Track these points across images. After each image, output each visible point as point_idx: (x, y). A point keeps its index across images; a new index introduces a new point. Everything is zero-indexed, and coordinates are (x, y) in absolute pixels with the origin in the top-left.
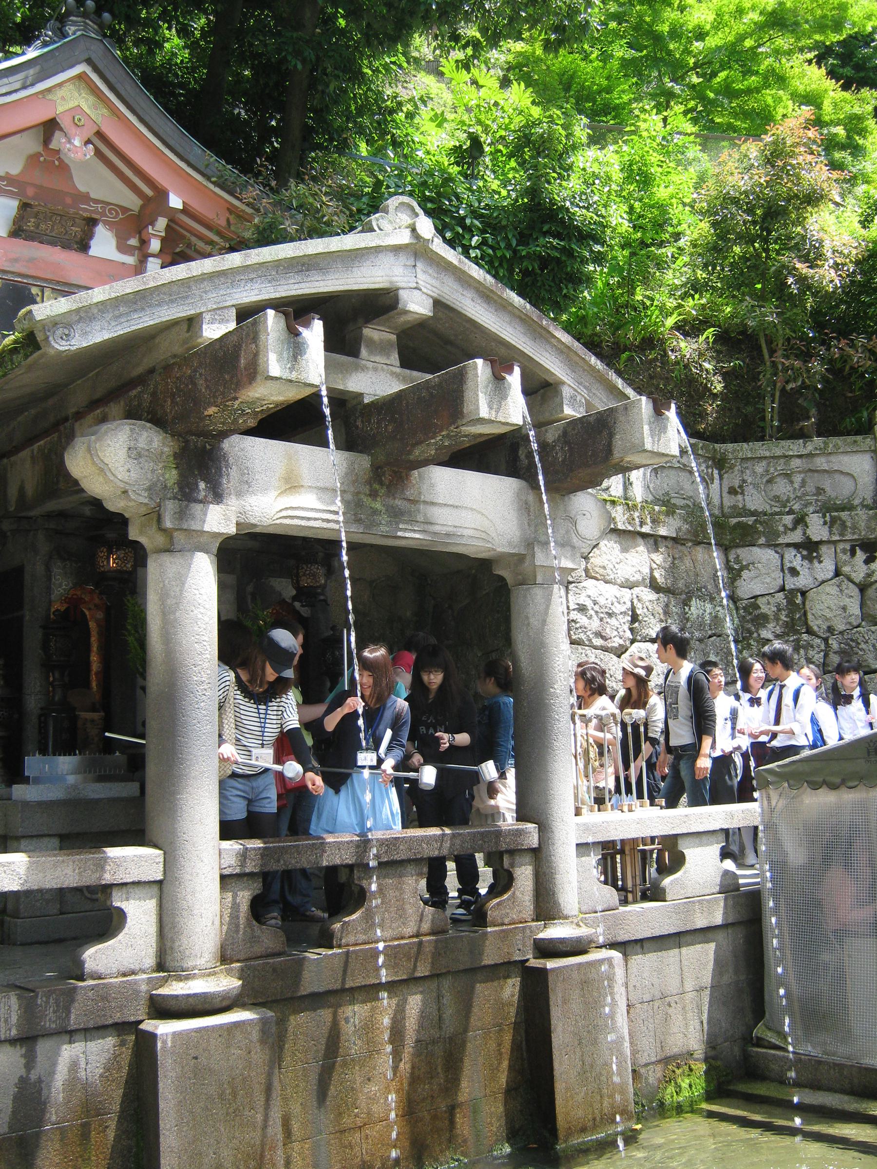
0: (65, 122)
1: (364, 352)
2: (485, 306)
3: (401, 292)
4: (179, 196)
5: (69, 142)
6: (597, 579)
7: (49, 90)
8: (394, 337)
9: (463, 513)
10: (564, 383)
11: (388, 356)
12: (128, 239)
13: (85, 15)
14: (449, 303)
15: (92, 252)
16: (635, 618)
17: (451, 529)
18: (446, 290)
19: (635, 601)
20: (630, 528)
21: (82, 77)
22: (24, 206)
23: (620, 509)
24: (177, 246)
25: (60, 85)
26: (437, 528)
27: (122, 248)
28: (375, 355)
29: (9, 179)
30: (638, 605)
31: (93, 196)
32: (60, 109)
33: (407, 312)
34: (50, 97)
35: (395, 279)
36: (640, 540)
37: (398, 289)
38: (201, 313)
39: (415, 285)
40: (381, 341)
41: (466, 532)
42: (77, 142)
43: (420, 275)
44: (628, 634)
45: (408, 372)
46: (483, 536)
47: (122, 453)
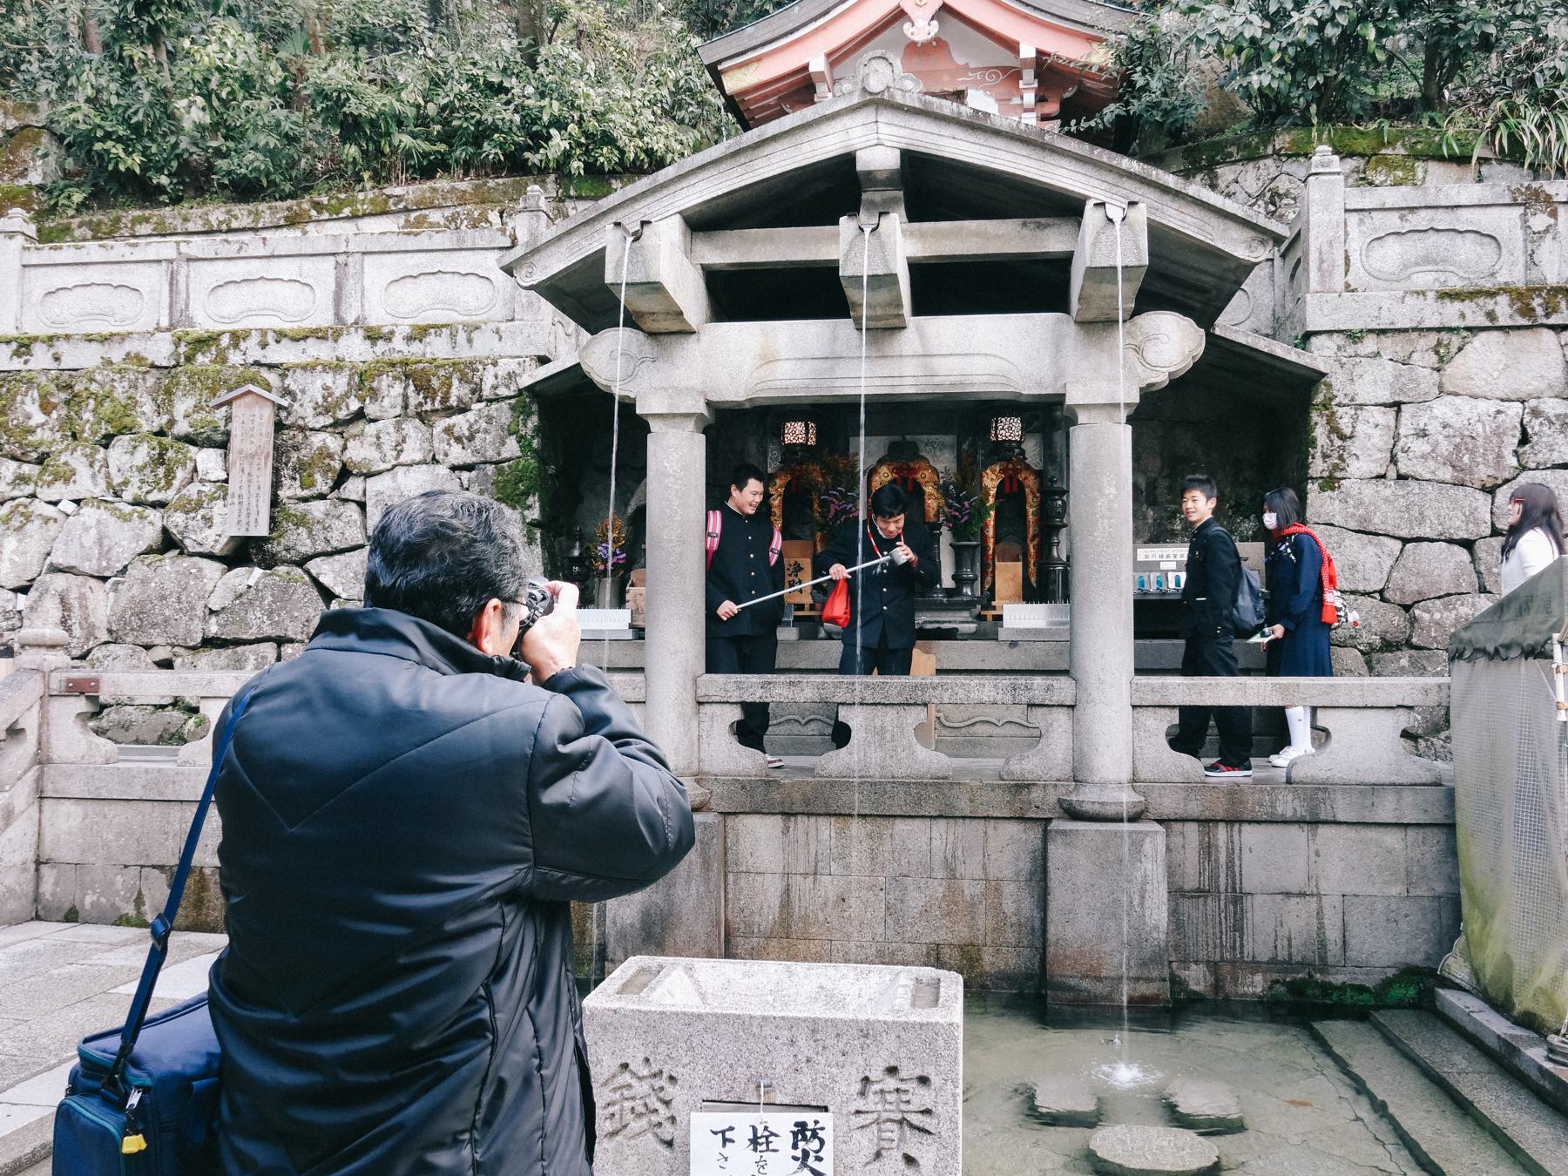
3: (858, 154)
6: (1457, 394)
9: (976, 360)
16: (1525, 439)
18: (919, 136)
19: (1527, 419)
20: (1524, 322)
23: (1503, 300)
26: (937, 380)
30: (1534, 426)
33: (869, 173)
36: (1548, 335)
41: (976, 379)
43: (883, 128)
44: (1514, 462)
45: (916, 225)
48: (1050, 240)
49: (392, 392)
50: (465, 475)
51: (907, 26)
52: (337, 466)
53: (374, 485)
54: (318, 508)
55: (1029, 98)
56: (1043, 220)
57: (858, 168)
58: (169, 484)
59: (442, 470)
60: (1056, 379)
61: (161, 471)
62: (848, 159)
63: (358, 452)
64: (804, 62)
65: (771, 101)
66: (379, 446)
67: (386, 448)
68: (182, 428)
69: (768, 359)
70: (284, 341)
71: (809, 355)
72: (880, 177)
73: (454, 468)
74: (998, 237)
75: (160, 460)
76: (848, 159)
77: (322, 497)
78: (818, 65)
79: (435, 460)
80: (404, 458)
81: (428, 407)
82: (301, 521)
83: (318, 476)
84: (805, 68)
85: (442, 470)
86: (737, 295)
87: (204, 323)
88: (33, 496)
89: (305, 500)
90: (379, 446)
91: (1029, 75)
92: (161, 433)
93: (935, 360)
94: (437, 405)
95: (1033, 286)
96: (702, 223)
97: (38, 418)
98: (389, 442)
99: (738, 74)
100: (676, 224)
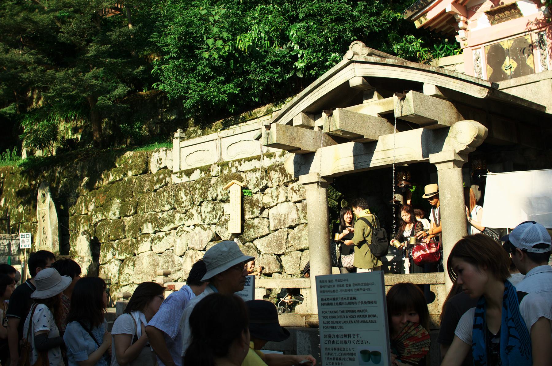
49: (275, 175)
50: (298, 204)
52: (262, 206)
53: (271, 211)
54: (256, 221)
58: (216, 217)
59: (291, 203)
61: (214, 213)
62: (347, 82)
63: (266, 199)
66: (272, 197)
67: (274, 197)
68: (220, 197)
70: (246, 162)
73: (295, 203)
75: (214, 209)
76: (347, 82)
77: (257, 217)
78: (449, 8)
79: (289, 201)
80: (280, 201)
81: (285, 181)
82: (253, 227)
83: (255, 210)
84: (445, 10)
85: (291, 203)
87: (226, 159)
88: (184, 225)
89: (253, 218)
90: (272, 197)
92: (215, 200)
94: (289, 180)
97: (184, 198)
98: (275, 194)
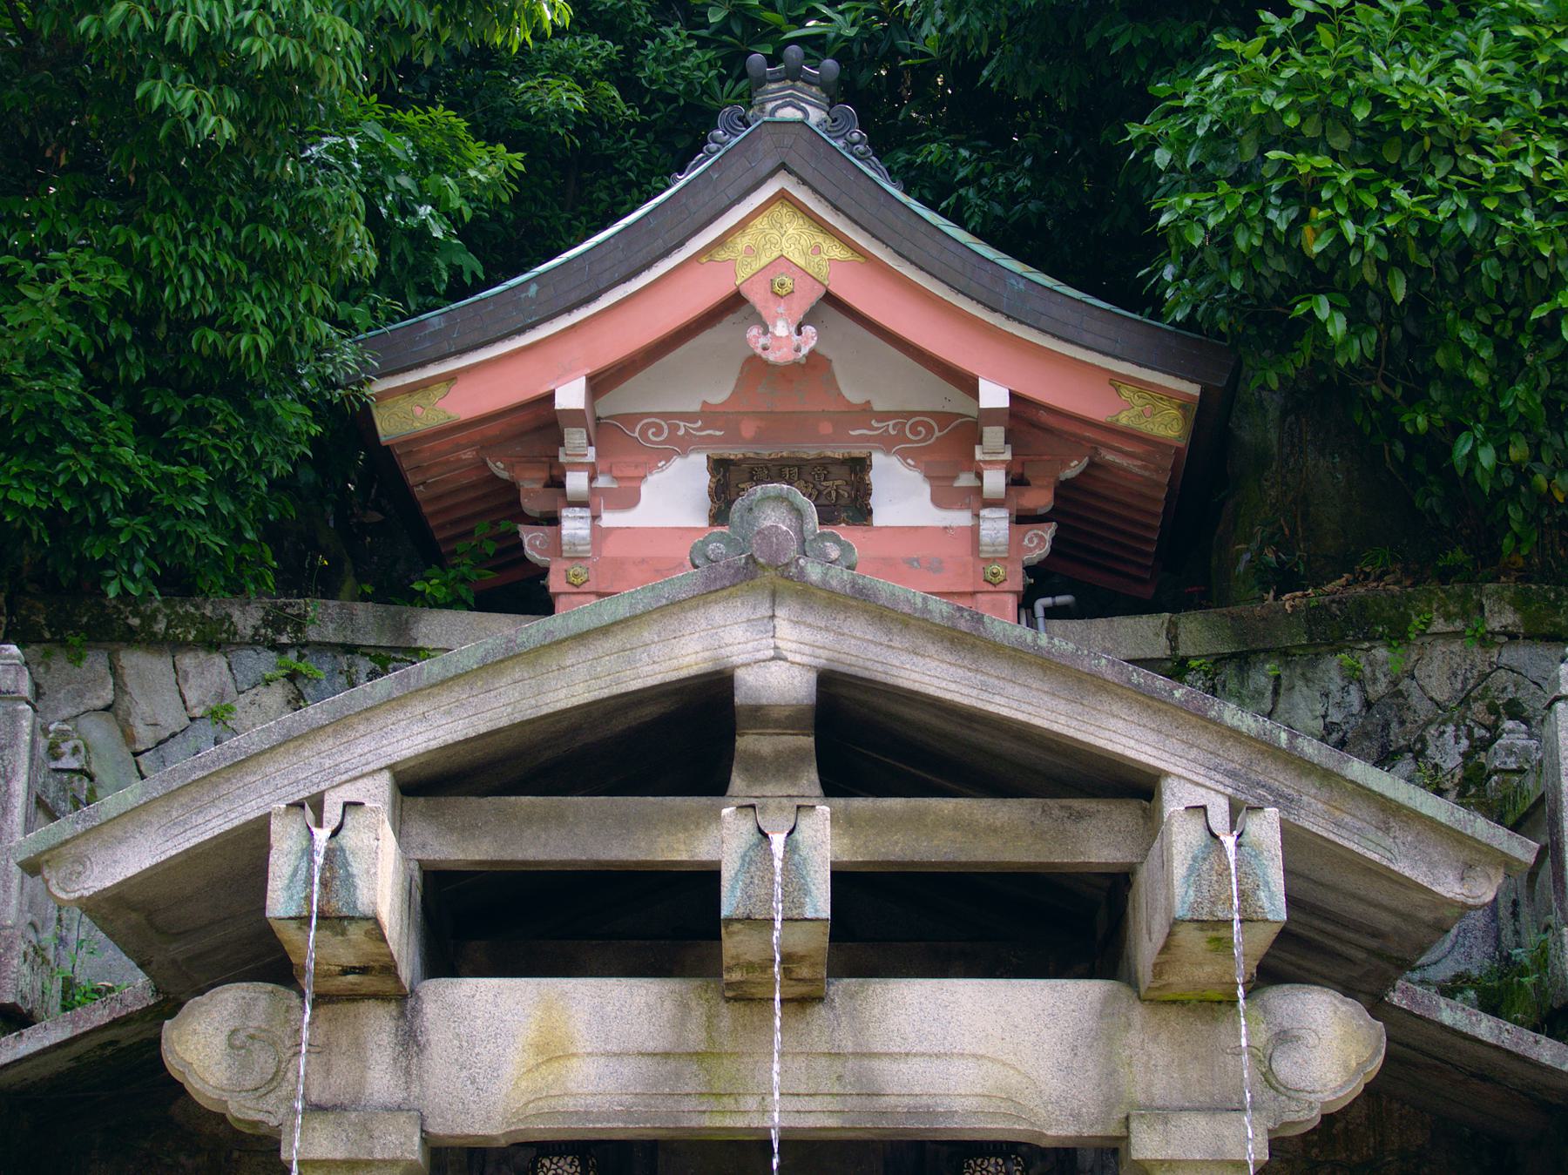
0: (757, 296)
1: (737, 782)
2: (950, 658)
4: (996, 379)
5: (766, 332)
7: (720, 242)
8: (808, 742)
9: (957, 1067)
10: (1167, 774)
11: (793, 779)
12: (955, 478)
13: (794, 75)
14: (852, 671)
15: (879, 519)
17: (925, 1100)
21: (782, 196)
22: (719, 467)
24: (1065, 464)
25: (742, 225)
27: (942, 499)
28: (763, 783)
29: (708, 415)
31: (878, 406)
32: (743, 274)
34: (723, 255)
35: (725, 652)
37: (734, 668)
38: (323, 793)
39: (771, 653)
40: (778, 755)
41: (957, 1105)
42: (782, 329)
46: (1004, 1107)
47: (220, 1041)
48: (1094, 840)
51: (754, 331)
55: (995, 481)
56: (1077, 804)
57: (737, 700)
60: (1109, 1104)
64: (544, 389)
65: (468, 455)
69: (550, 1051)
71: (631, 1046)
72: (775, 714)
74: (994, 830)
78: (571, 396)
84: (550, 397)
86: (484, 923)
91: (994, 436)
93: (875, 1064)
95: (1059, 925)
96: (423, 786)
99: (403, 404)
100: (377, 793)
